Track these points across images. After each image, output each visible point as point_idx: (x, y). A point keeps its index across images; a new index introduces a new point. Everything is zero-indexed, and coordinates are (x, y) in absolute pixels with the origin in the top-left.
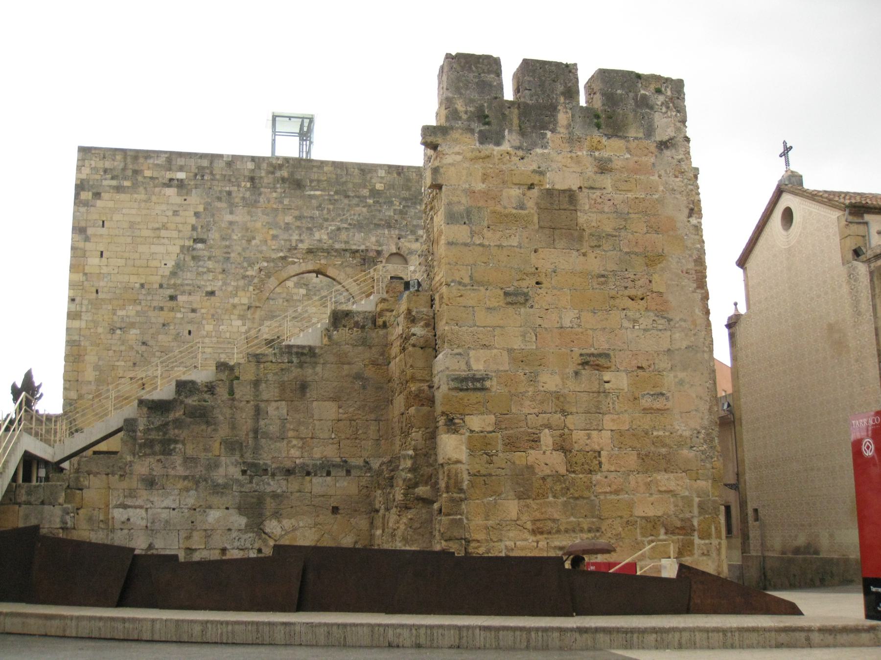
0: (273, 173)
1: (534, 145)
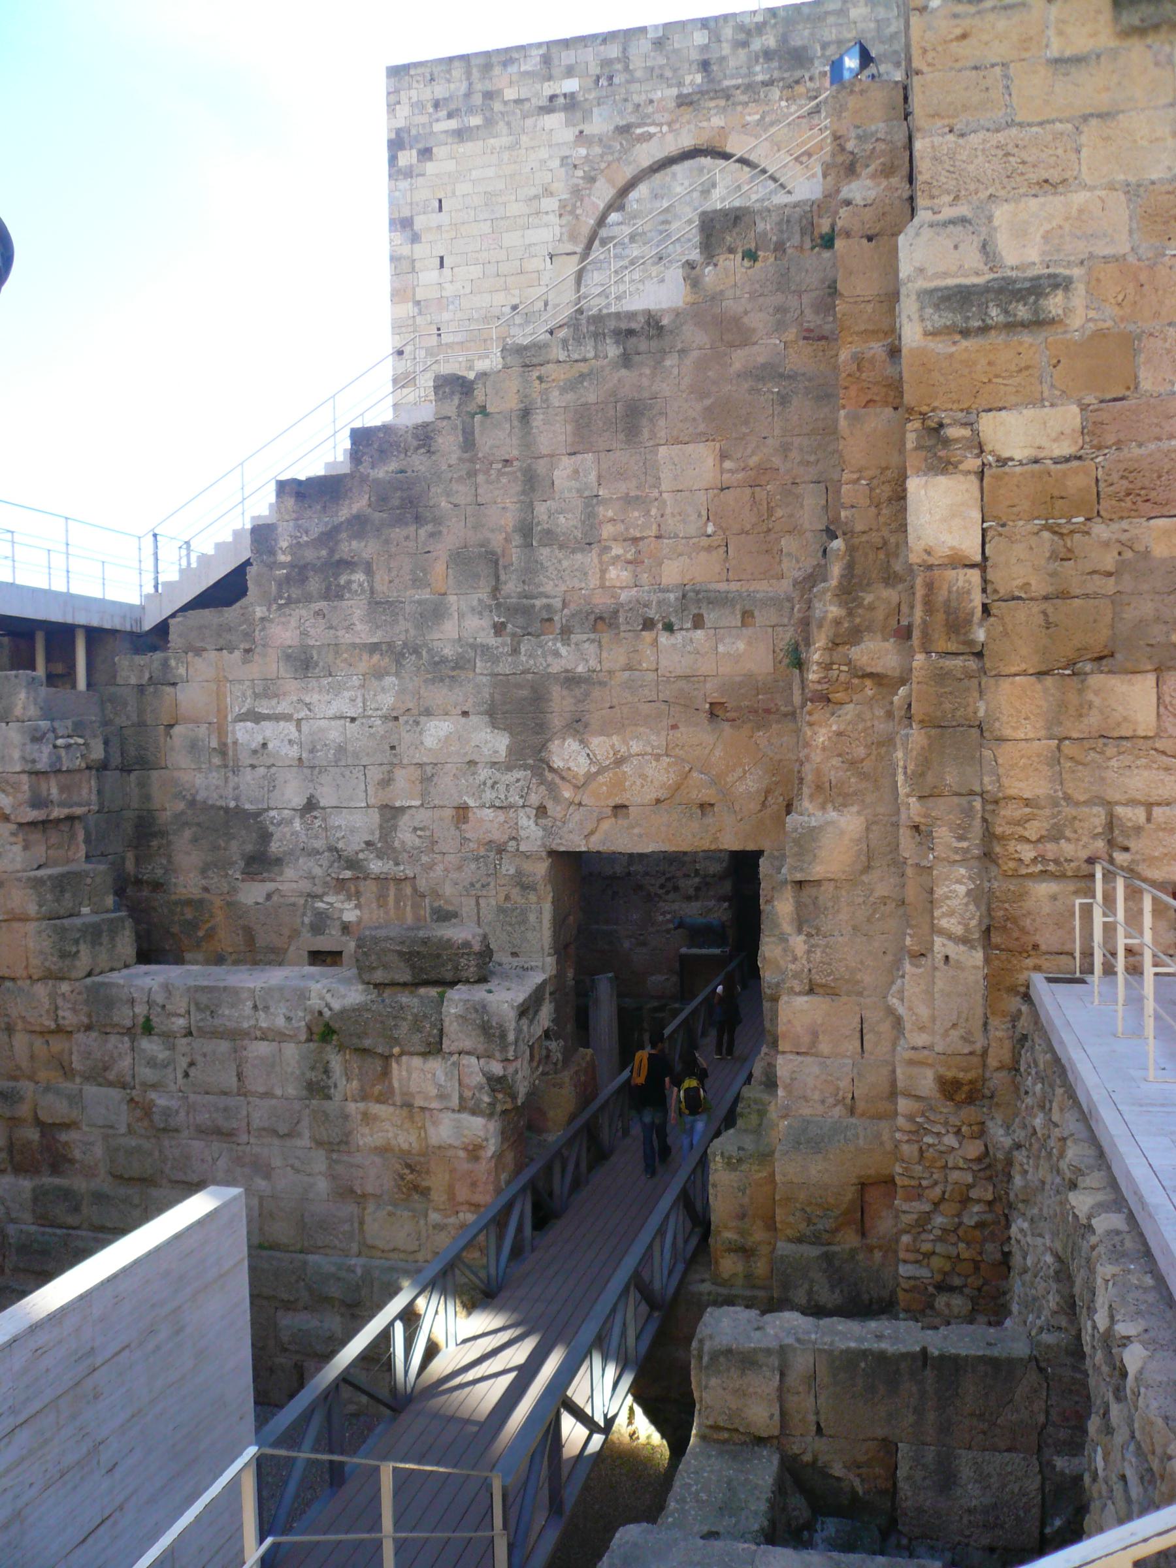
0: (745, 44)
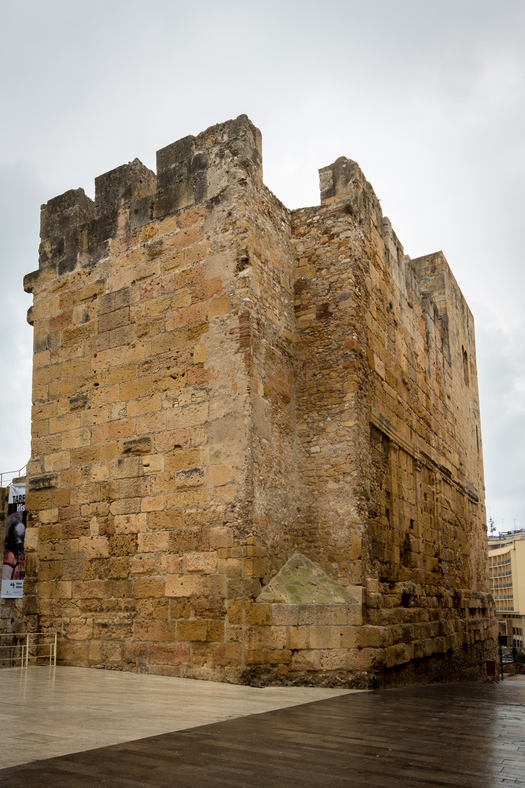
1: (99, 257)
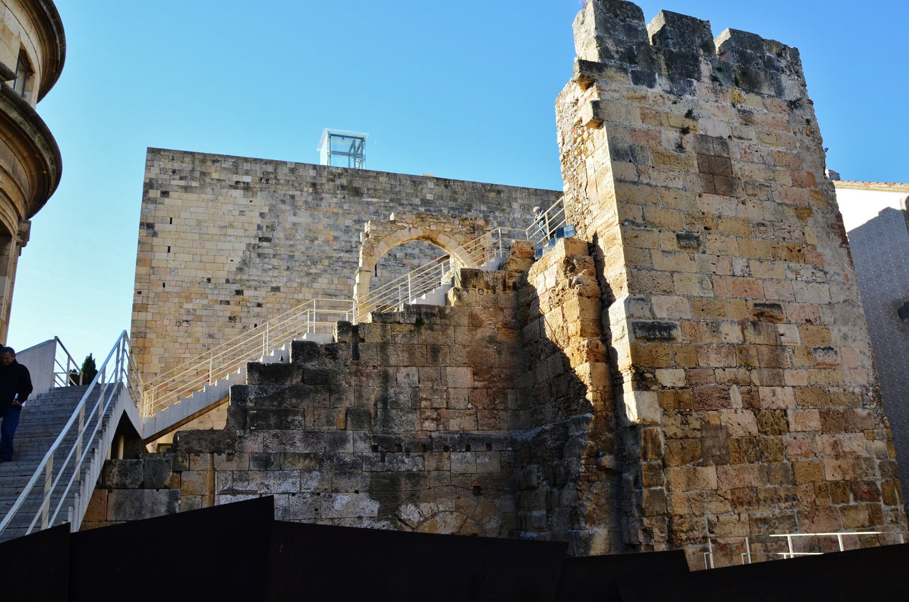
1: (684, 91)
